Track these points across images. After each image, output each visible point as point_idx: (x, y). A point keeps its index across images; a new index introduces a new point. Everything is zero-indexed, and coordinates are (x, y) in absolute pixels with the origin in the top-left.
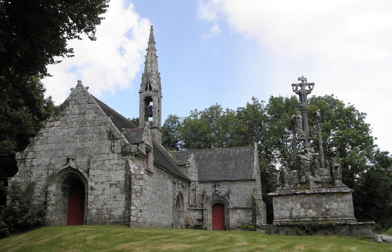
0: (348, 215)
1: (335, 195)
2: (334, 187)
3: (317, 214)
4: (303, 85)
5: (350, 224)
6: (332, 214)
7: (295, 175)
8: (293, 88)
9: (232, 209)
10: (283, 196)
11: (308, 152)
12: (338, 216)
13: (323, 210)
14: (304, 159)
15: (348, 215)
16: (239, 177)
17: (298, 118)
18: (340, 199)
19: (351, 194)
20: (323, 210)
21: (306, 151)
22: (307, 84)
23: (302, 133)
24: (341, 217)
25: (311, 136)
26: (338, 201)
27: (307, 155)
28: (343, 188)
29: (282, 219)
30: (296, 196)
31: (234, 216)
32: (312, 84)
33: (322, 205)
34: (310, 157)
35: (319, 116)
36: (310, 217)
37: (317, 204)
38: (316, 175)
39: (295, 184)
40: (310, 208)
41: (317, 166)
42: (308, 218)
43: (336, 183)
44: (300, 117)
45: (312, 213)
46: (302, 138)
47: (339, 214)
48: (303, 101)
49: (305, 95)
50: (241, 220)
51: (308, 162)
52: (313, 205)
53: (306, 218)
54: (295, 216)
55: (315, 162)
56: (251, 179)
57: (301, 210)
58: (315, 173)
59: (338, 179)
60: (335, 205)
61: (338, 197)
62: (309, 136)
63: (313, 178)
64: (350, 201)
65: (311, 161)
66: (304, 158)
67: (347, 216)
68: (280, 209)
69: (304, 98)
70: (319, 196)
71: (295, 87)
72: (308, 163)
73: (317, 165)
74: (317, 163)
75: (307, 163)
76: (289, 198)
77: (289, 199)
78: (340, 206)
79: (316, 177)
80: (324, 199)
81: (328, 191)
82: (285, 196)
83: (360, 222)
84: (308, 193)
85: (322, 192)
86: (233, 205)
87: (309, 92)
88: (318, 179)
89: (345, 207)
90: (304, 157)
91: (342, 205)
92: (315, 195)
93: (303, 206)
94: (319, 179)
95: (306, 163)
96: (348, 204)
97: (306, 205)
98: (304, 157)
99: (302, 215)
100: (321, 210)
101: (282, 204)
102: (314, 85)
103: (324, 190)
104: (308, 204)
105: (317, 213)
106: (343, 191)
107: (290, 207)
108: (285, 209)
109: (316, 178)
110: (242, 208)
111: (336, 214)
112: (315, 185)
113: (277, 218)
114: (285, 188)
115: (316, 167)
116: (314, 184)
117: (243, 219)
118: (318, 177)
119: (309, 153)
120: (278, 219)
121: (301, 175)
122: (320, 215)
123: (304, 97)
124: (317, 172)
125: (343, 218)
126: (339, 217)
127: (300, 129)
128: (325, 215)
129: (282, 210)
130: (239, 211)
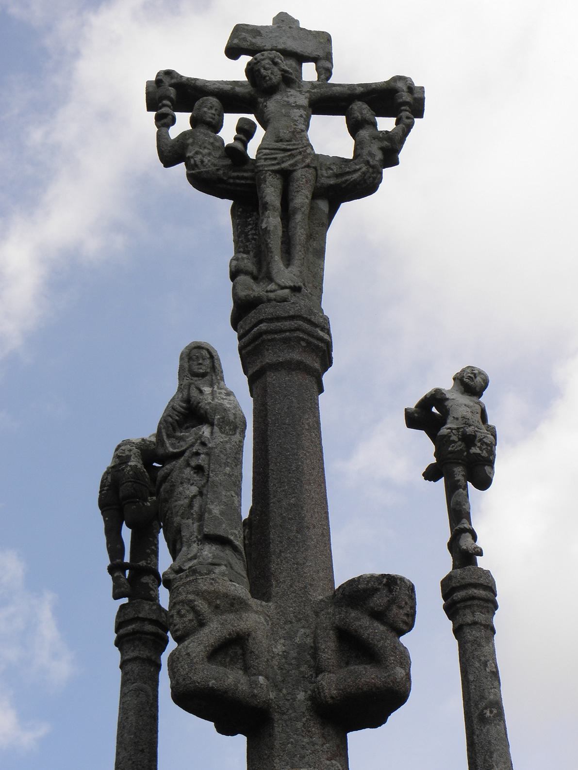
23: (235, 605)
48: (275, 243)
87: (356, 181)
127: (208, 551)
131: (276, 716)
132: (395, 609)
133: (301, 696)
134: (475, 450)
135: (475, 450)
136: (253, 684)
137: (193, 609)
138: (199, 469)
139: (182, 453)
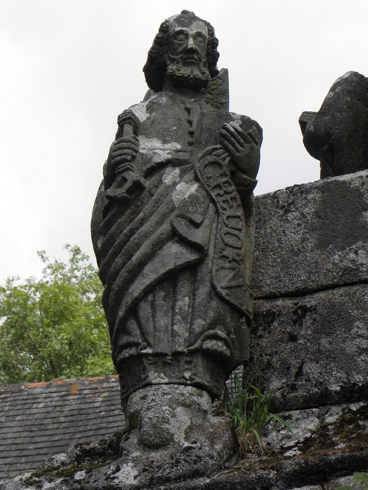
39: (349, 394)
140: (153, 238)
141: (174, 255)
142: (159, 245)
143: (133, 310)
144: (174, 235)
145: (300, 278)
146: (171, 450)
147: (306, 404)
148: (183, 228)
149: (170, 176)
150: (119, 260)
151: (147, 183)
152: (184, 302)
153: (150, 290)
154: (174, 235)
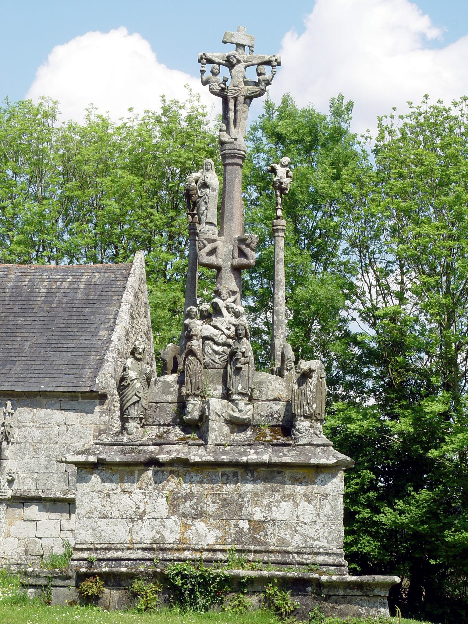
0: (322, 548)
1: (288, 473)
2: (289, 445)
3: (221, 538)
4: (239, 62)
5: (318, 580)
6: (271, 542)
7: (169, 393)
8: (203, 72)
9: (8, 500)
10: (115, 468)
11: (224, 311)
12: (289, 549)
13: (244, 525)
14: (205, 338)
15: (322, 548)
16: (47, 380)
17: (205, 185)
18: (300, 489)
19: (341, 474)
20: (244, 525)
21: (217, 311)
22: (255, 62)
23: (214, 241)
24: (298, 553)
25: (242, 254)
26: (296, 494)
27: (218, 324)
28: (318, 450)
29: (101, 549)
30: (157, 468)
31: (13, 529)
32: (268, 63)
33: (242, 506)
34: (226, 332)
35: (281, 183)
36: (196, 547)
37: (225, 503)
38: (235, 397)
40: (201, 515)
41: (245, 364)
42: (189, 550)
43: (297, 430)
44: (213, 179)
45: (206, 534)
46: (212, 260)
47: (295, 542)
48: (232, 121)
49: (241, 99)
50: (39, 546)
51: (216, 348)
52: (211, 508)
53: (184, 549)
54: (148, 542)
55: (239, 353)
56: (88, 389)
57: (168, 522)
58: (234, 390)
59: (307, 417)
60: (282, 511)
61: (297, 480)
62: (236, 253)
63: (224, 406)
64: (335, 499)
65: (229, 346)
66: (206, 333)
67: (321, 550)
68: (96, 514)
69: (235, 112)
70: (235, 474)
71: (208, 67)
72: (216, 353)
73: (243, 360)
74: (243, 353)
75: (214, 351)
76: (132, 473)
77: (131, 478)
78: (300, 513)
79: (237, 405)
80: (250, 487)
81: (266, 458)
82: (121, 468)
83: (390, 573)
84: (198, 459)
85: (244, 459)
86: (15, 486)
88: (241, 411)
89: (315, 519)
90: (208, 330)
91: (307, 511)
92: (221, 470)
93: (175, 506)
94: (245, 410)
95: (211, 351)
96: (327, 509)
97: (188, 504)
98: (208, 330)
99: (170, 539)
100: (236, 525)
101: (109, 495)
102: (279, 64)
103: (252, 456)
104: (195, 500)
105: (220, 534)
106: (313, 461)
107: (134, 507)
108: (115, 513)
109: (234, 407)
110: (45, 500)
111: (282, 541)
112: (232, 432)
113: (84, 546)
114: (125, 440)
115: (240, 369)
116: (226, 429)
117: (46, 542)
118: (242, 404)
119: (228, 317)
120: (88, 549)
121: (188, 396)
122: (229, 541)
123: (235, 106)
124: (240, 387)
125: (306, 556)
126: (291, 553)
128: (245, 546)
129: (104, 517)
130: (33, 511)
131: (223, 268)
132: (252, 244)
133: (229, 264)
134: (283, 186)
135: (283, 186)
136: (218, 261)
137: (203, 243)
138: (206, 202)
139: (202, 197)
140: (132, 395)
141: (135, 399)
142: (133, 396)
143: (127, 409)
144: (136, 395)
145: (157, 400)
146: (133, 436)
147: (156, 425)
148: (137, 394)
149: (135, 381)
150: (125, 398)
151: (131, 383)
152: (136, 408)
153: (131, 405)
154: (136, 395)
